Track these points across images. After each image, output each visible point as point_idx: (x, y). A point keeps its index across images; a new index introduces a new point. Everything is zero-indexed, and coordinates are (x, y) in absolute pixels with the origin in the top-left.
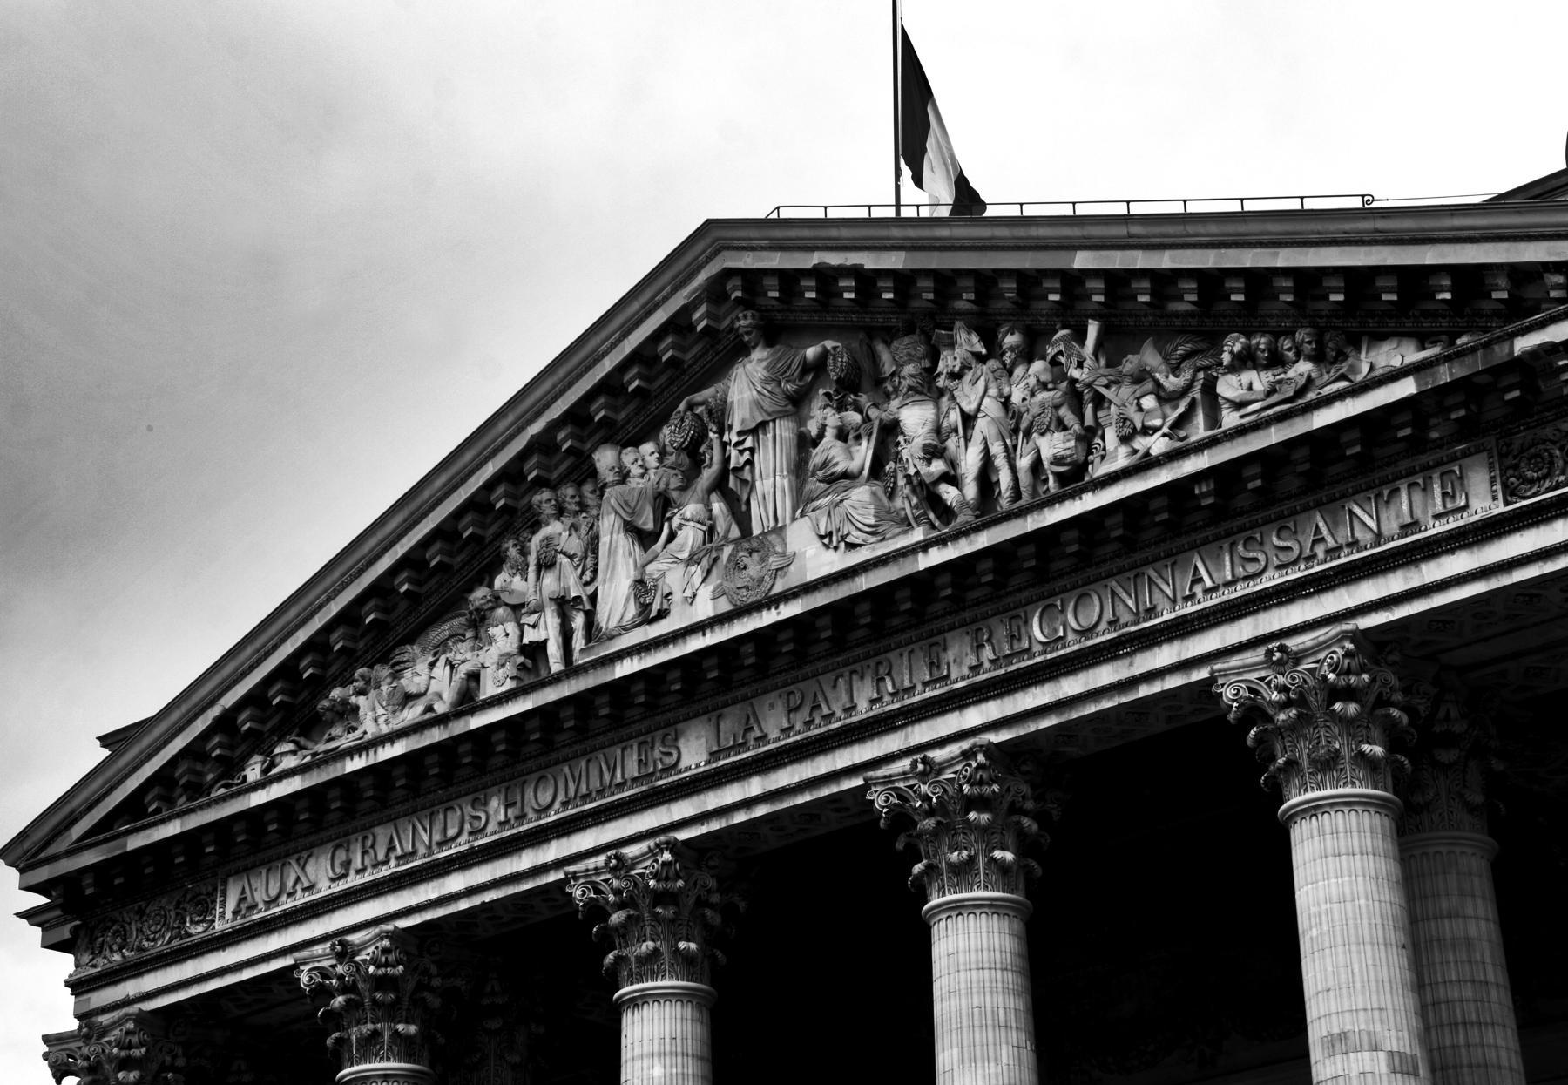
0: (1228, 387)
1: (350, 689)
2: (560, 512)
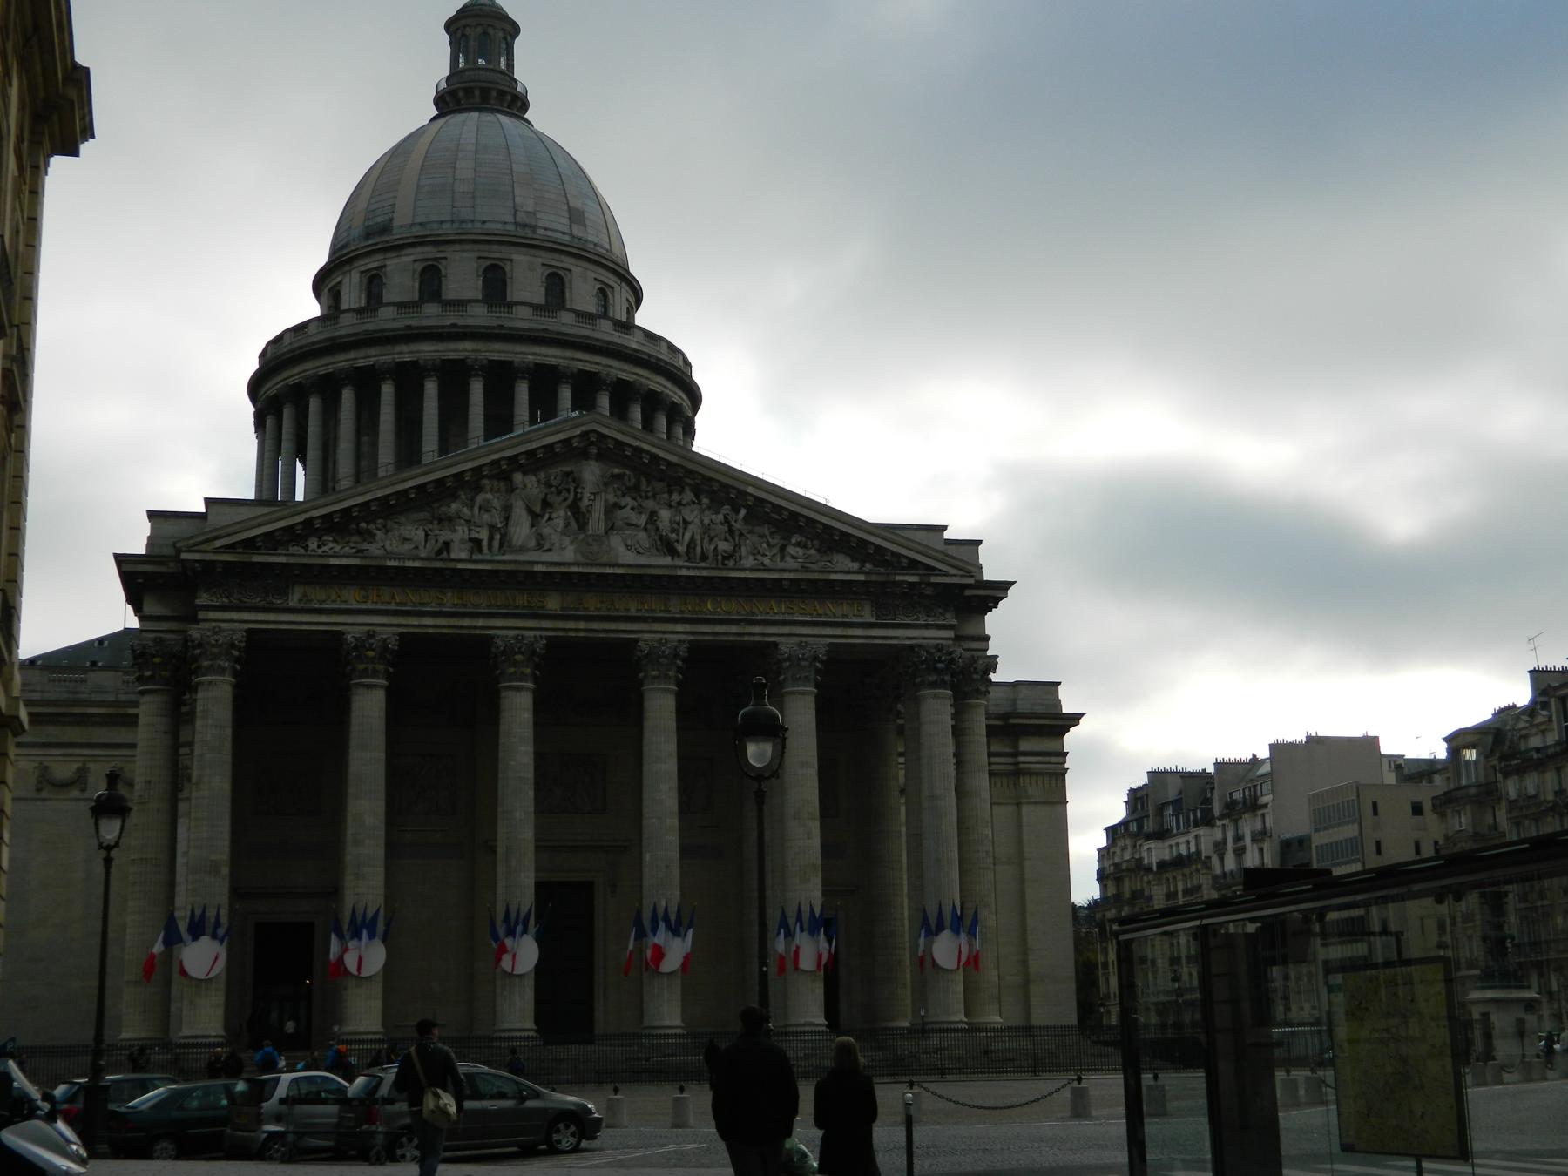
0: (791, 550)
1: (372, 526)
2: (491, 490)
